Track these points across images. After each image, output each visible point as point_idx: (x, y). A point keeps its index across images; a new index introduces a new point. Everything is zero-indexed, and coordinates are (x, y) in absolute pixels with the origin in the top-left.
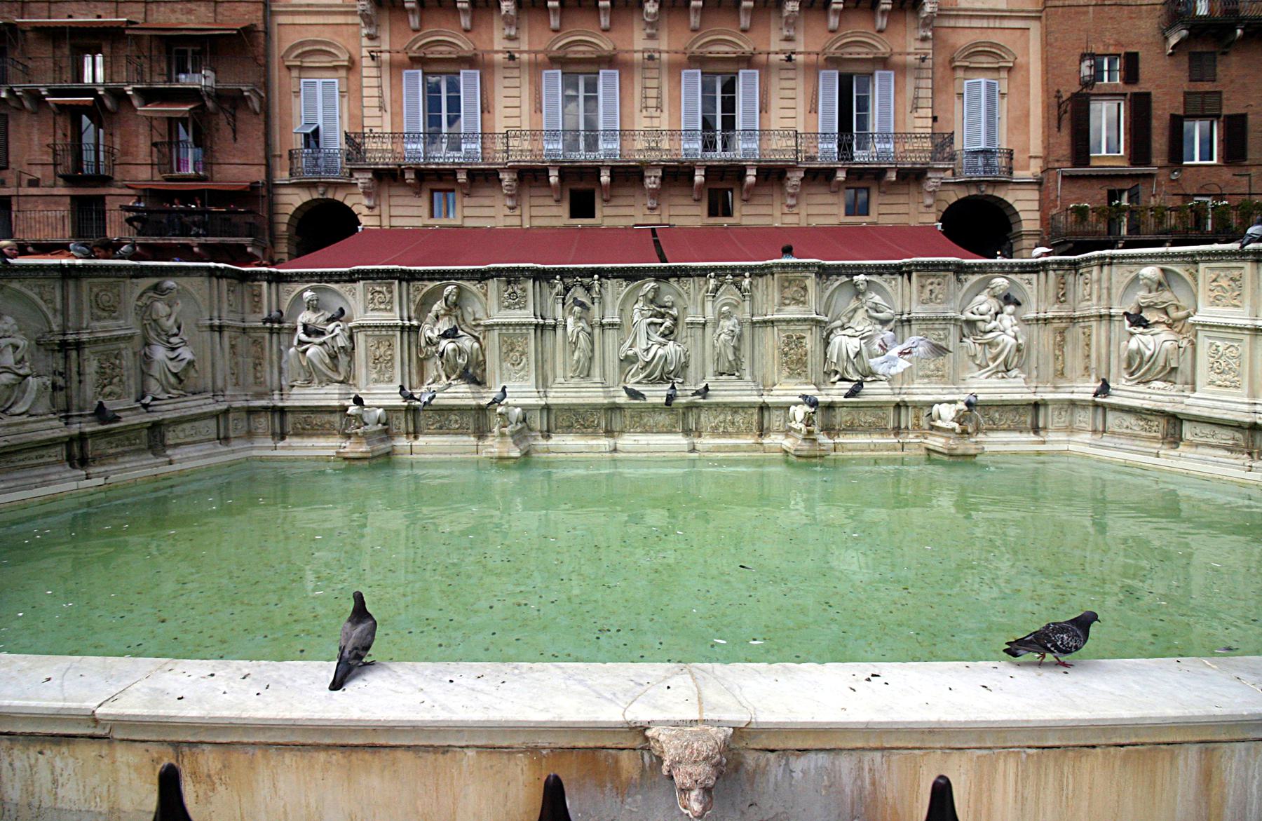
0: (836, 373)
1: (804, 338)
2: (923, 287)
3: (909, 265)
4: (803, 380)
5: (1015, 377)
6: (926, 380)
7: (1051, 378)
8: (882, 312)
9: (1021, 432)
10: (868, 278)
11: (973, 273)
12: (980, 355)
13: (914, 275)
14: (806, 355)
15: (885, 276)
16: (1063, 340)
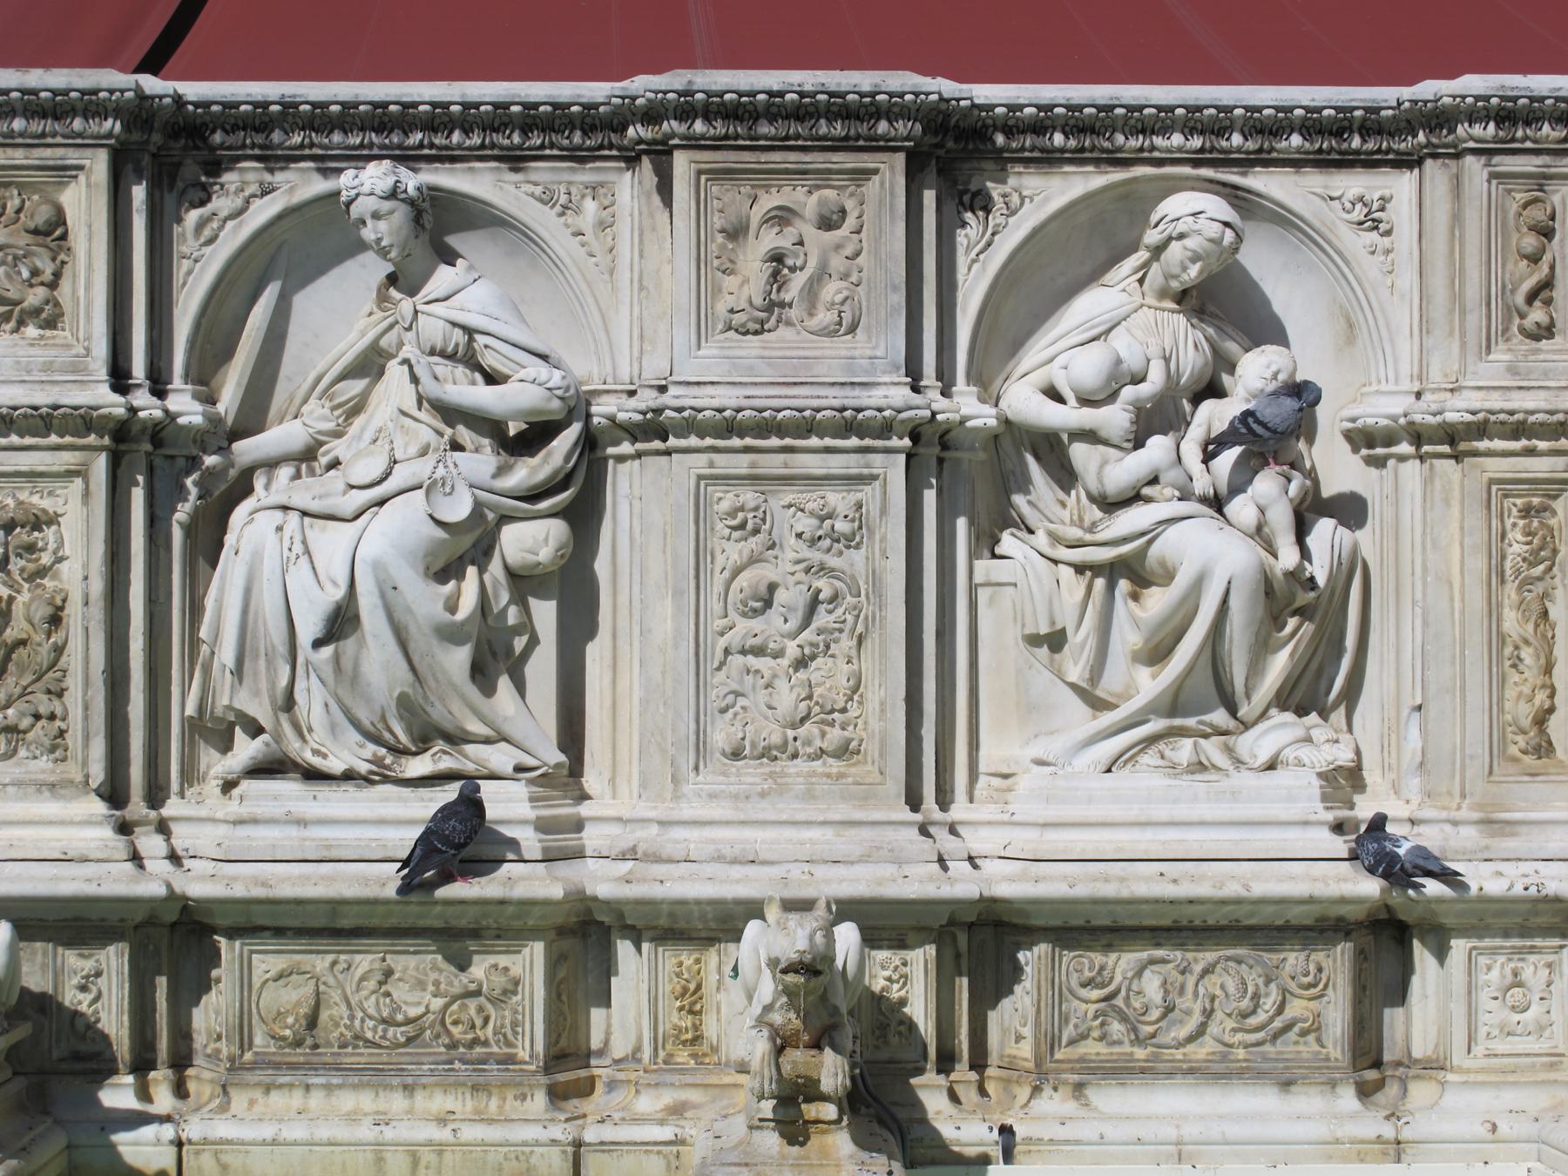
0: (255, 730)
1: (53, 520)
2: (736, 233)
3: (652, 115)
4: (43, 766)
5: (1271, 766)
6: (751, 774)
7: (1477, 768)
8: (492, 378)
9: (1286, 1085)
10: (412, 181)
11: (1049, 160)
12: (1082, 637)
13: (682, 164)
14: (55, 620)
15: (542, 172)
16: (1543, 552)
